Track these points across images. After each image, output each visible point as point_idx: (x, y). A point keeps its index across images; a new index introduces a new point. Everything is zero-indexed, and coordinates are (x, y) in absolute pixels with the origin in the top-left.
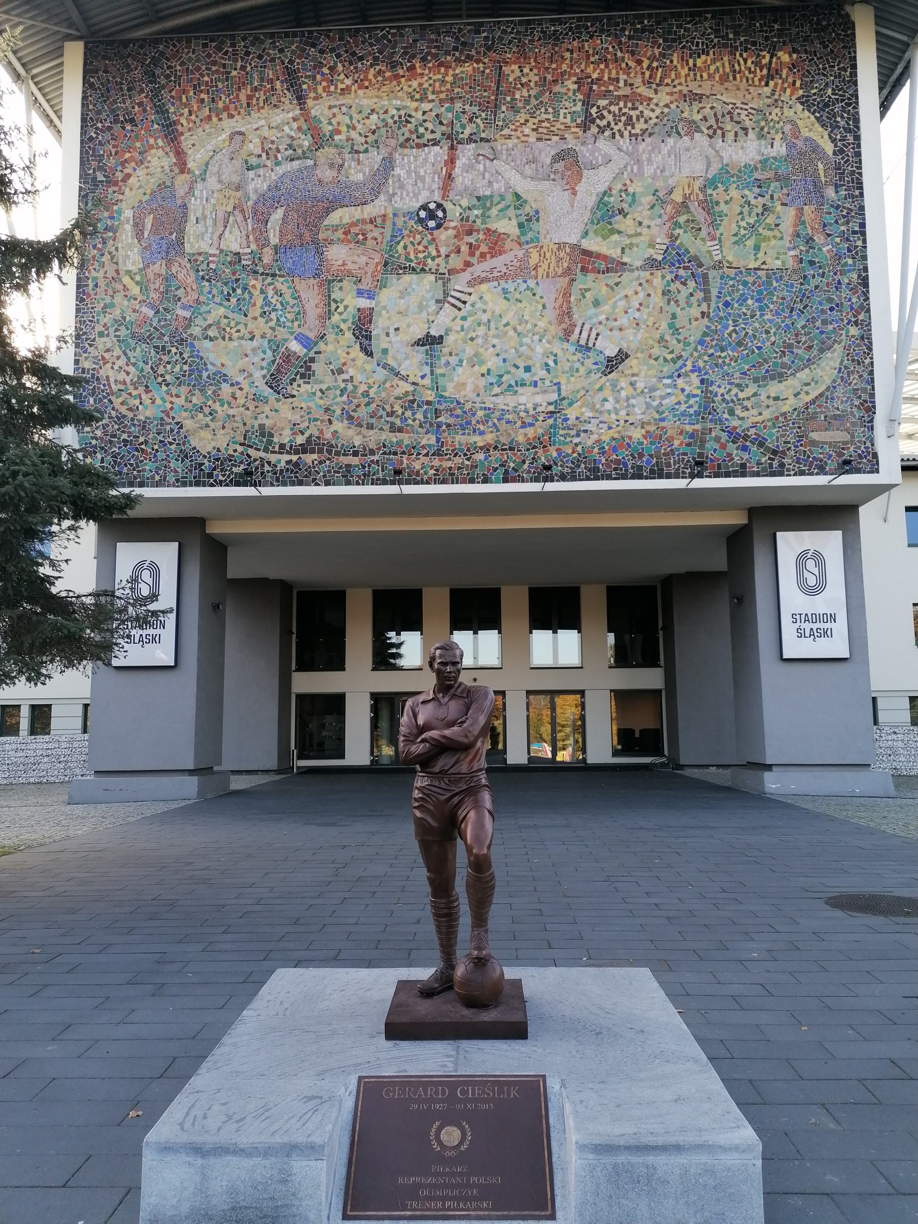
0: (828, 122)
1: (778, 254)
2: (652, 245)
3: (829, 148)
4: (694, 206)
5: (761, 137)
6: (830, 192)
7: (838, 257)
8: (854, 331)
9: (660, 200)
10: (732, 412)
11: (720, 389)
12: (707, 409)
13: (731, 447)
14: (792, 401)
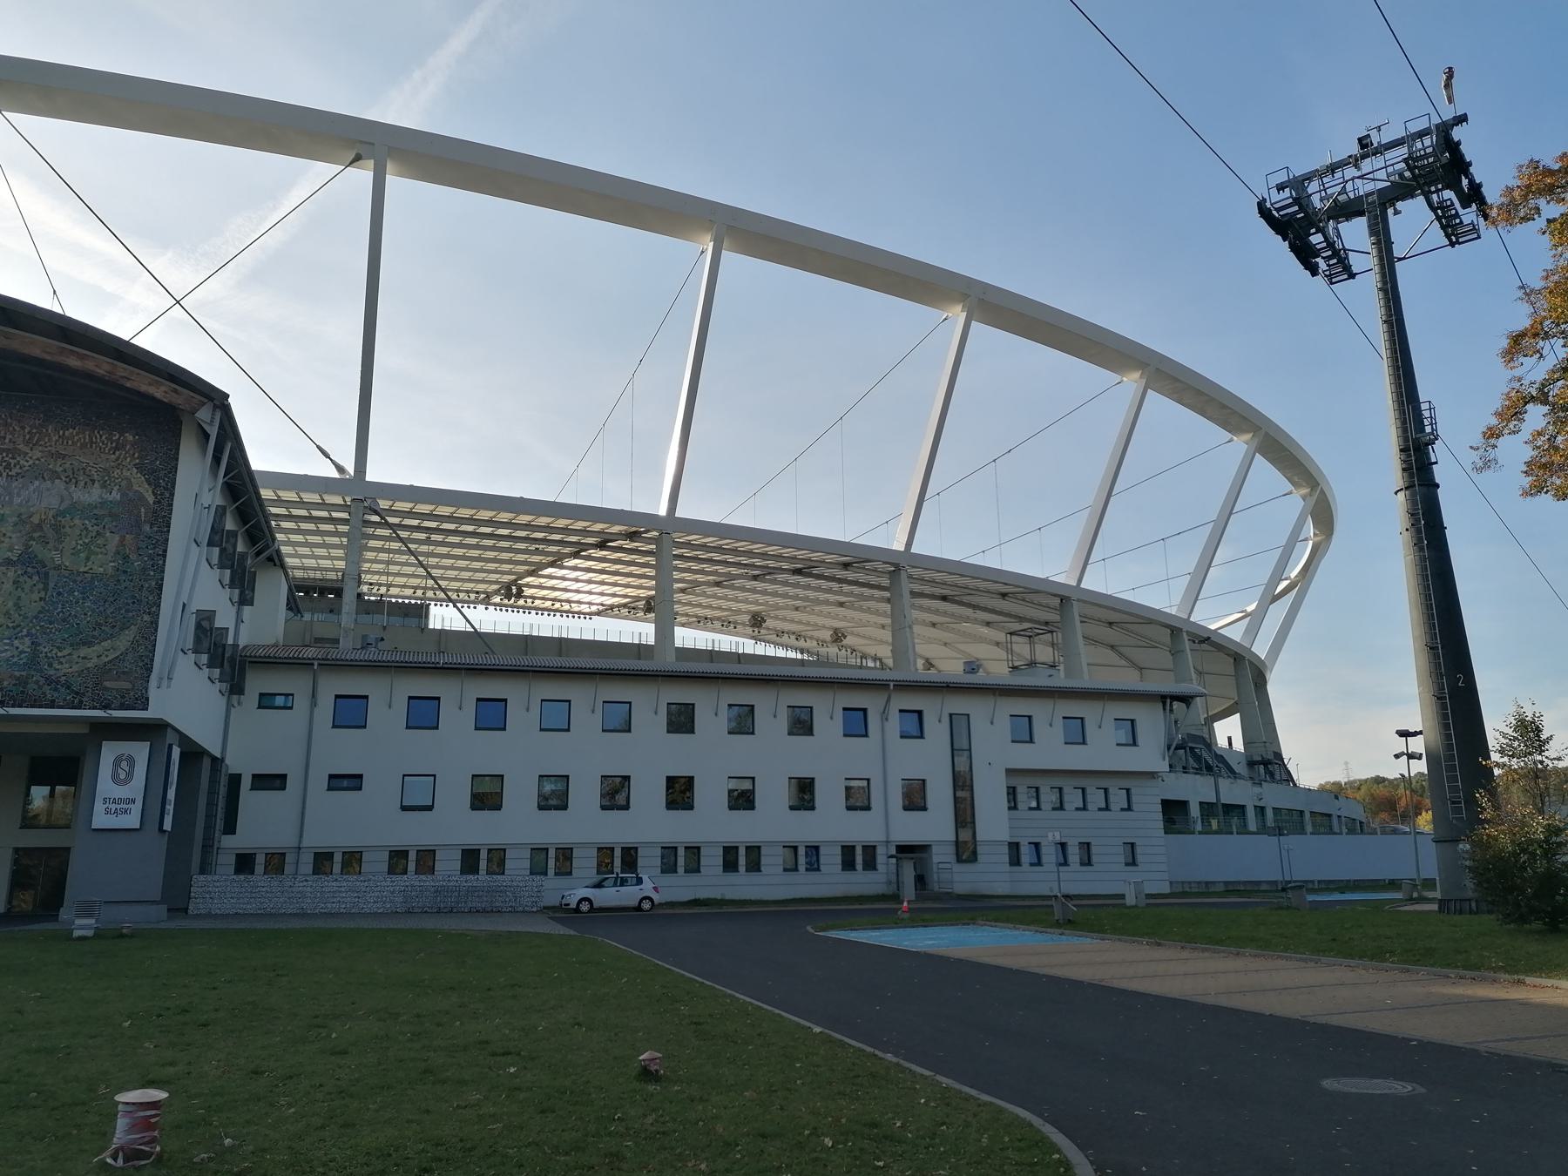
0: (154, 483)
1: (103, 564)
2: (11, 549)
3: (151, 499)
4: (46, 527)
5: (103, 486)
6: (147, 528)
7: (144, 570)
8: (146, 618)
9: (22, 521)
10: (50, 665)
11: (45, 649)
12: (33, 661)
13: (47, 689)
14: (95, 660)
